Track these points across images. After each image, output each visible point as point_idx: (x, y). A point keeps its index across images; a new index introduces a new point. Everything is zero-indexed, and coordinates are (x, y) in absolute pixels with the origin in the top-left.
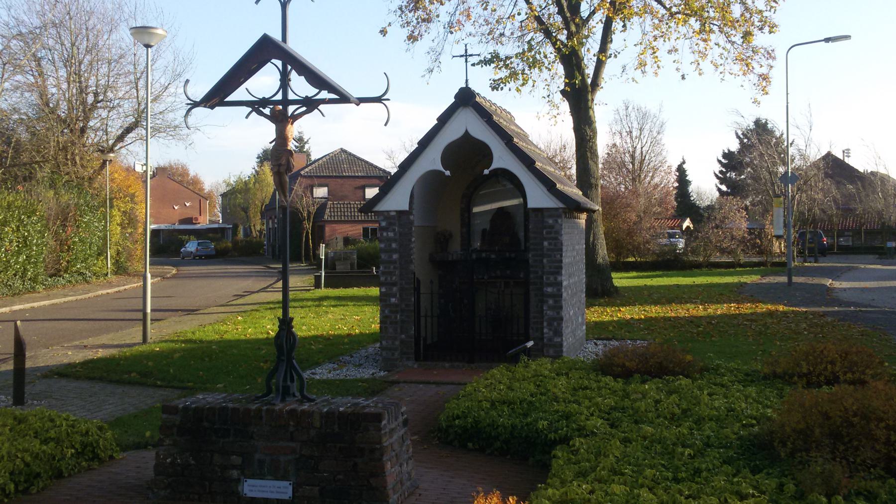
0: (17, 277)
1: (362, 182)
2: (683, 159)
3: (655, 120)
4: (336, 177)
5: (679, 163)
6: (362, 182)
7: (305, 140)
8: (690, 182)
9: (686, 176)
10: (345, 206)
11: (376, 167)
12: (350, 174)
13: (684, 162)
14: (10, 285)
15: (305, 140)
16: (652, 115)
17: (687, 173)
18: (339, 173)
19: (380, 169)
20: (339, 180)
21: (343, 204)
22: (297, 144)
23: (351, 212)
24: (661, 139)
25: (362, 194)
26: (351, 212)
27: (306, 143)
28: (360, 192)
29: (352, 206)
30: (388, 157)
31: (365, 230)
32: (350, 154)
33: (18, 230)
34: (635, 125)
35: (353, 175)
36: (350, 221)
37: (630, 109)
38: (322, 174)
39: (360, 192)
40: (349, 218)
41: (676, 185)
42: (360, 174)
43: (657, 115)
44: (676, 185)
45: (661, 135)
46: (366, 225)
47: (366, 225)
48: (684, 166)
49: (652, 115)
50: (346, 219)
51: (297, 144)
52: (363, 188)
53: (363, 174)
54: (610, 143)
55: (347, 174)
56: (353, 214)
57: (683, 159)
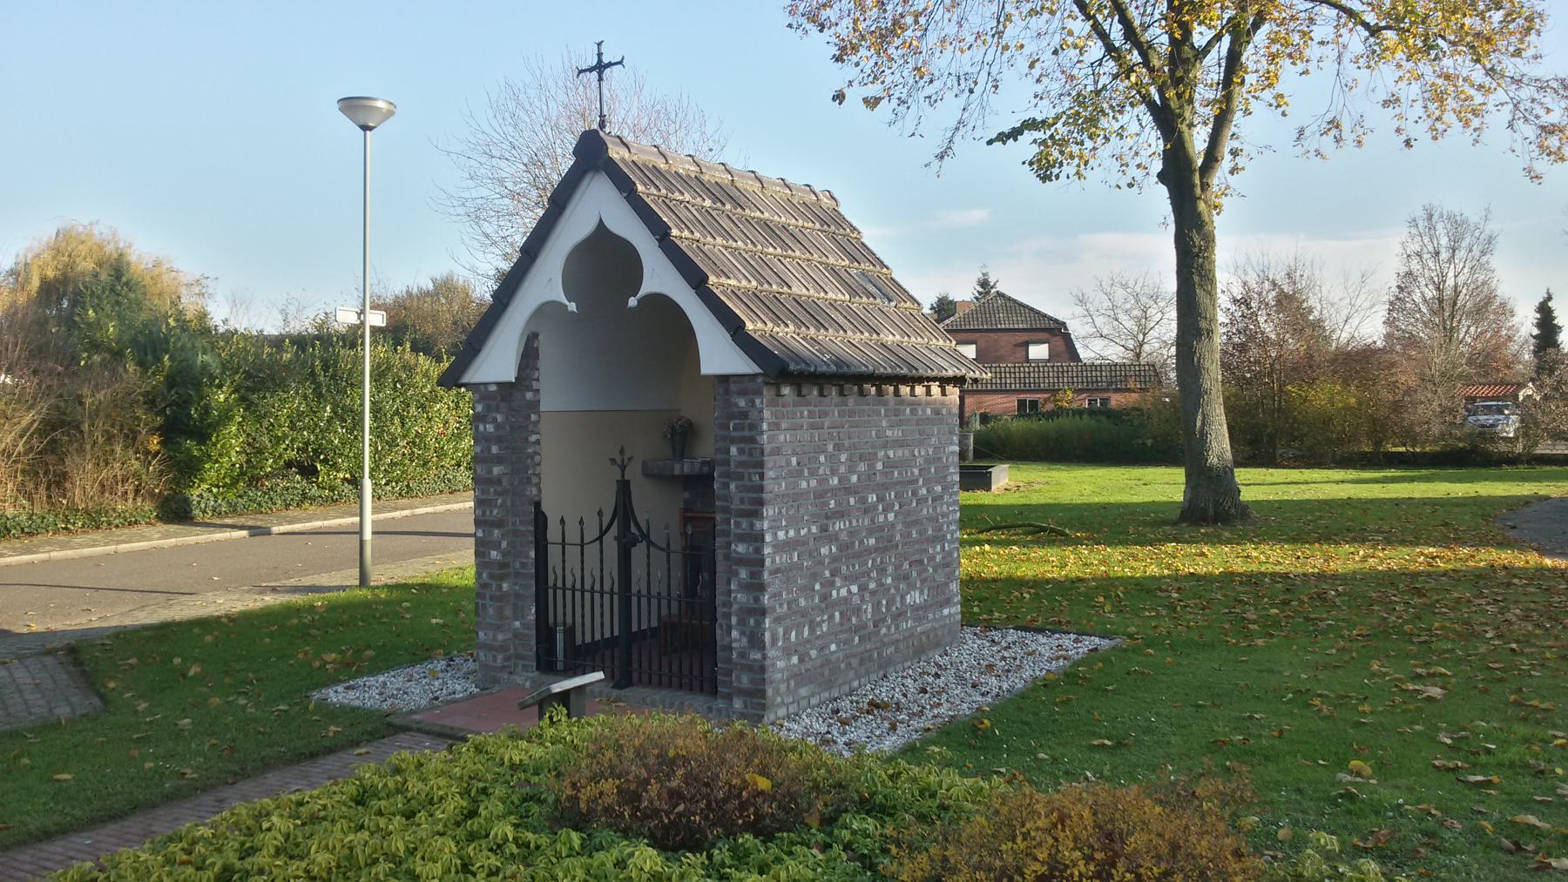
0: (462, 468)
1: (1025, 337)
2: (1548, 293)
3: (1477, 233)
4: (988, 331)
5: (1542, 300)
6: (1025, 337)
7: (992, 284)
8: (1560, 328)
9: (1554, 318)
10: (1007, 370)
11: (1045, 316)
12: (1007, 326)
13: (1550, 298)
14: (449, 480)
15: (992, 284)
16: (1472, 225)
17: (1555, 314)
18: (992, 325)
19: (1050, 319)
20: (992, 335)
21: (1053, 367)
22: (981, 290)
23: (1001, 378)
24: (1488, 263)
25: (1024, 353)
26: (1001, 378)
27: (992, 287)
28: (1020, 353)
29: (1003, 370)
30: (1077, 302)
31: (1021, 403)
32: (1010, 299)
33: (457, 407)
34: (1444, 241)
35: (1011, 326)
36: (1001, 391)
37: (1435, 218)
38: (968, 327)
39: (1020, 353)
40: (999, 386)
41: (1536, 332)
42: (1021, 326)
43: (1481, 227)
44: (1536, 332)
45: (1488, 256)
46: (1022, 396)
47: (1022, 396)
48: (1550, 304)
49: (1472, 225)
50: (994, 387)
51: (981, 290)
52: (1026, 344)
53: (1025, 326)
54: (1403, 270)
55: (1003, 326)
56: (1003, 381)
57: (1548, 293)
